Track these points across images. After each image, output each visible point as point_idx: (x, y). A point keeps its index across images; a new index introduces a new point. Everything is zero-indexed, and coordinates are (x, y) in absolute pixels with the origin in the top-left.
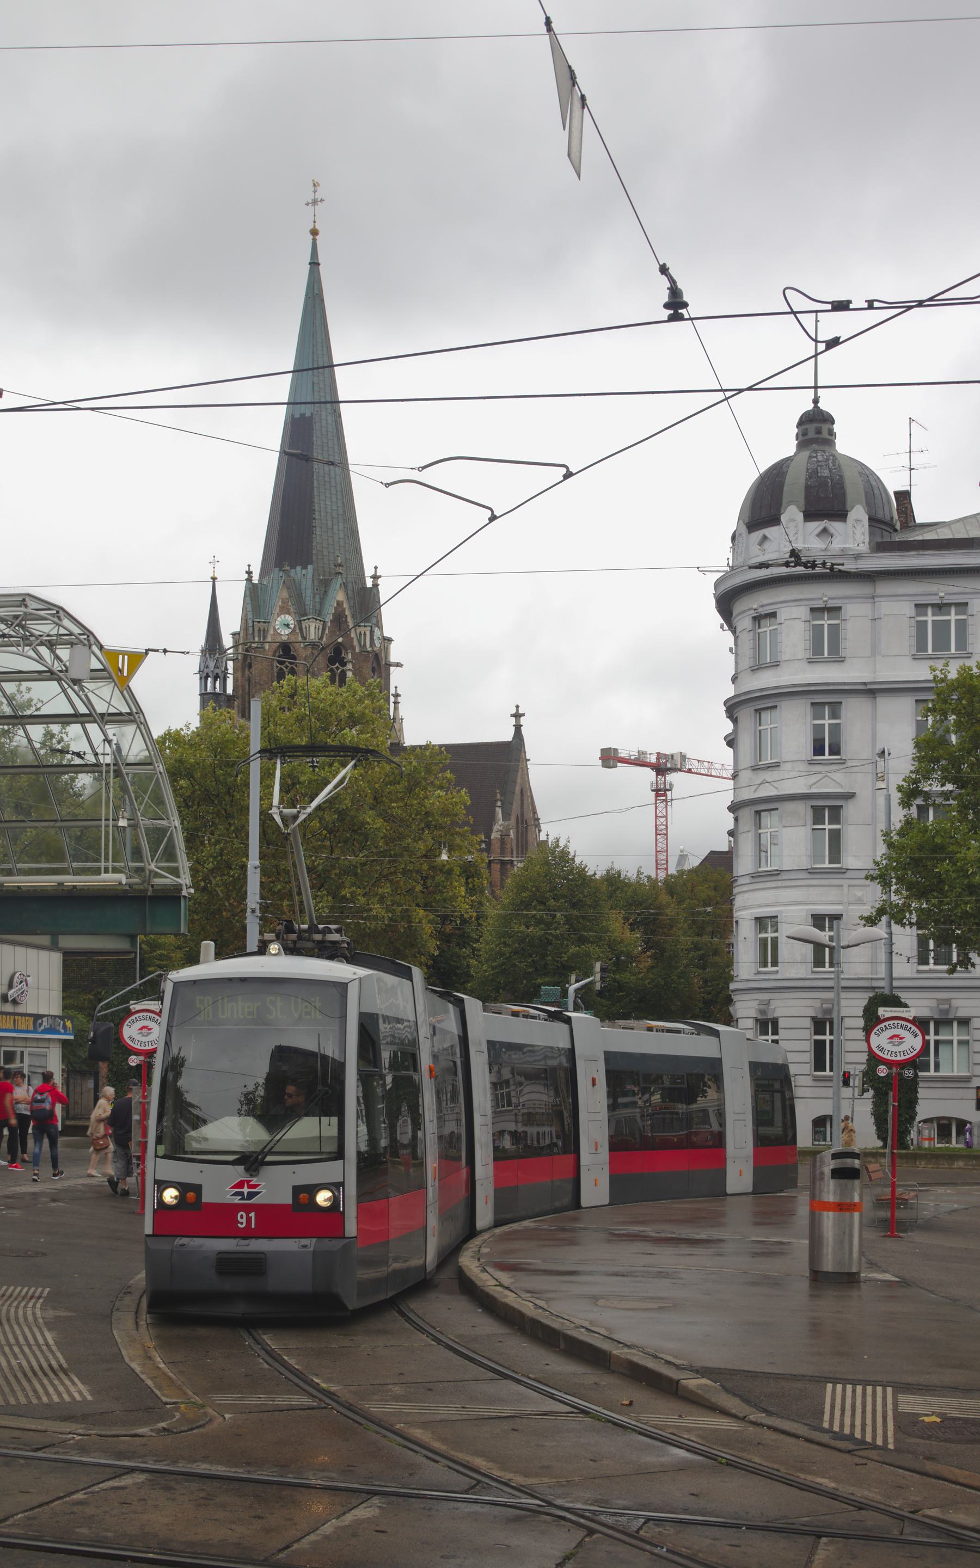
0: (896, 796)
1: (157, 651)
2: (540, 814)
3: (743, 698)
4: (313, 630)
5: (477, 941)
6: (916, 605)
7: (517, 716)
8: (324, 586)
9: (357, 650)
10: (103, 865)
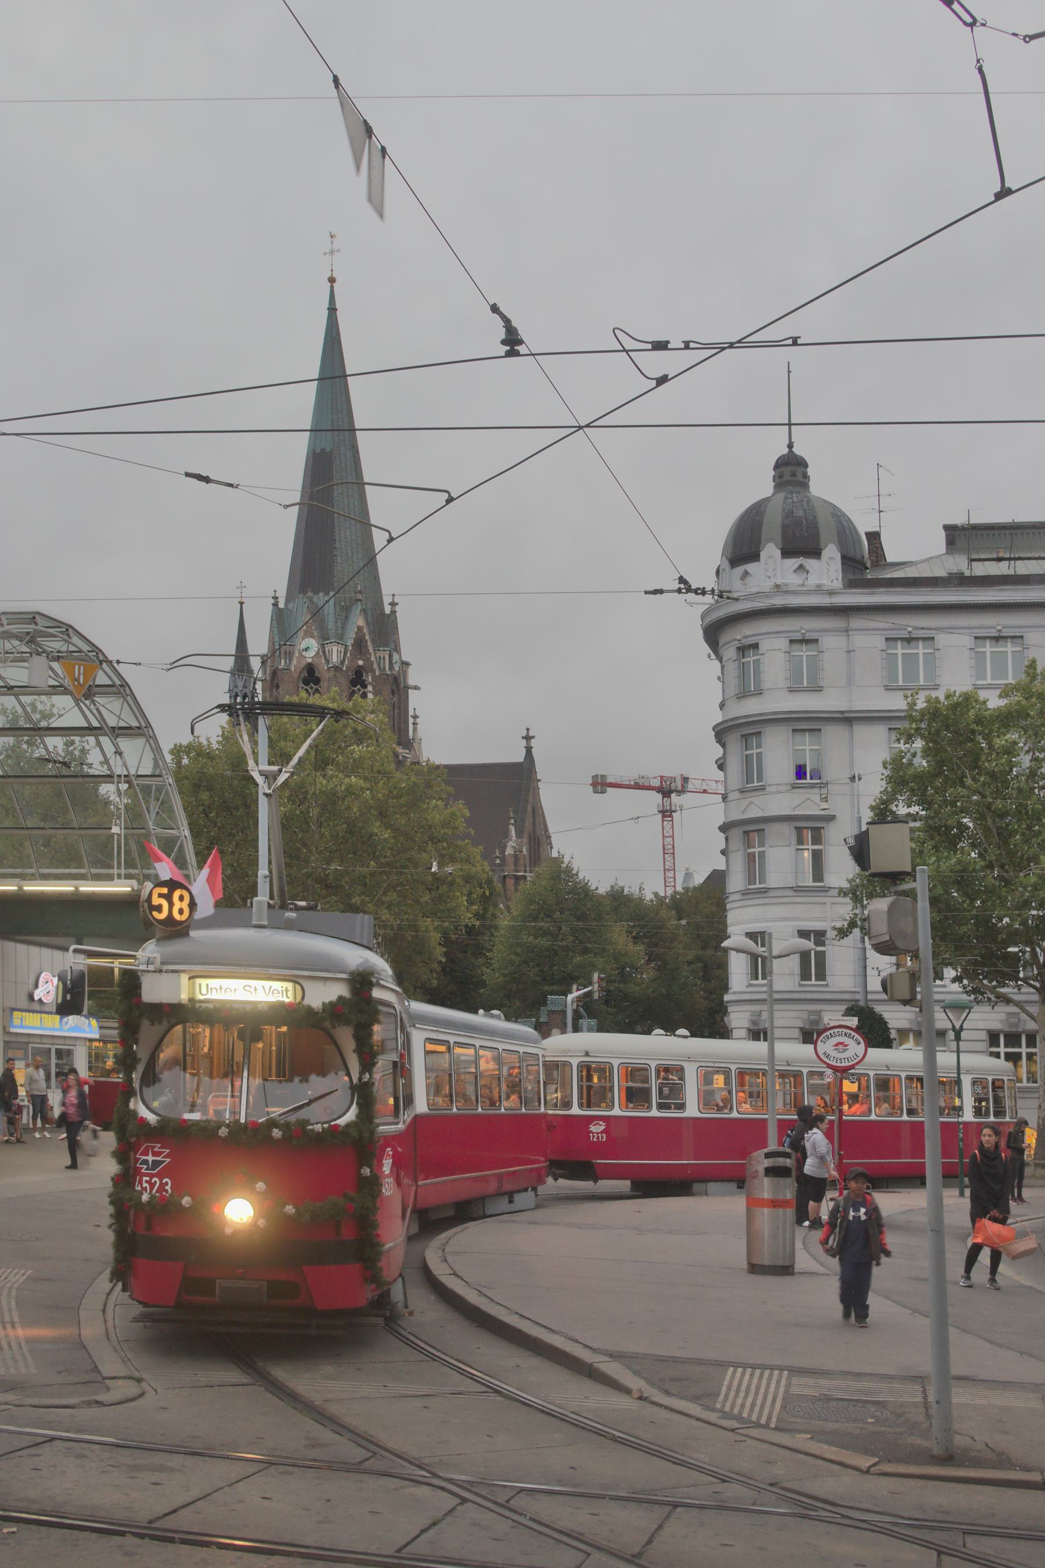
3: (730, 724)
4: (335, 654)
8: (345, 611)
9: (377, 673)
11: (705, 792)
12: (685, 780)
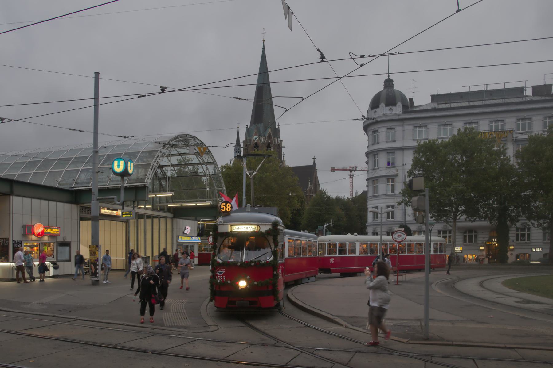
0: (407, 174)
1: (210, 146)
2: (320, 183)
3: (370, 152)
5: (303, 215)
6: (414, 127)
7: (314, 158)
8: (266, 129)
10: (206, 199)
11: (362, 170)
12: (356, 167)
